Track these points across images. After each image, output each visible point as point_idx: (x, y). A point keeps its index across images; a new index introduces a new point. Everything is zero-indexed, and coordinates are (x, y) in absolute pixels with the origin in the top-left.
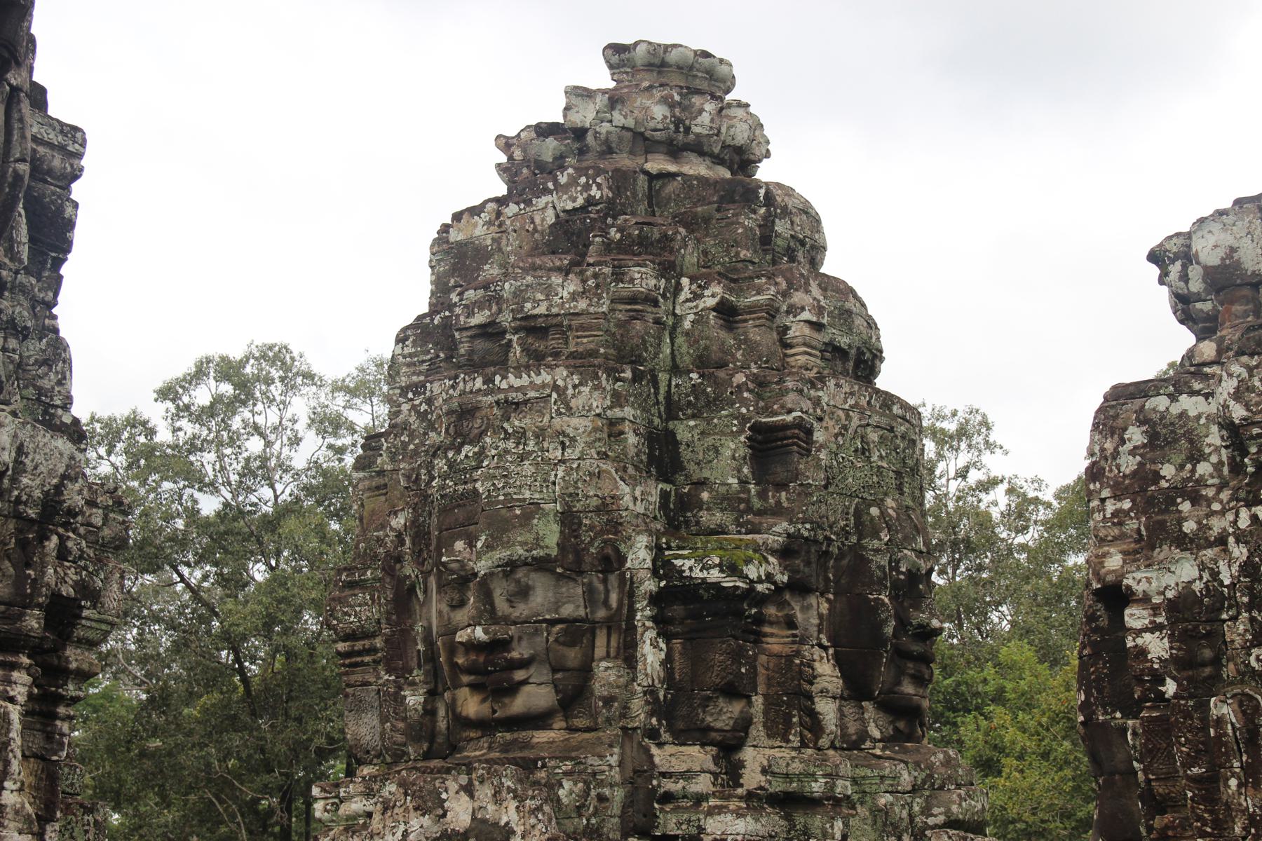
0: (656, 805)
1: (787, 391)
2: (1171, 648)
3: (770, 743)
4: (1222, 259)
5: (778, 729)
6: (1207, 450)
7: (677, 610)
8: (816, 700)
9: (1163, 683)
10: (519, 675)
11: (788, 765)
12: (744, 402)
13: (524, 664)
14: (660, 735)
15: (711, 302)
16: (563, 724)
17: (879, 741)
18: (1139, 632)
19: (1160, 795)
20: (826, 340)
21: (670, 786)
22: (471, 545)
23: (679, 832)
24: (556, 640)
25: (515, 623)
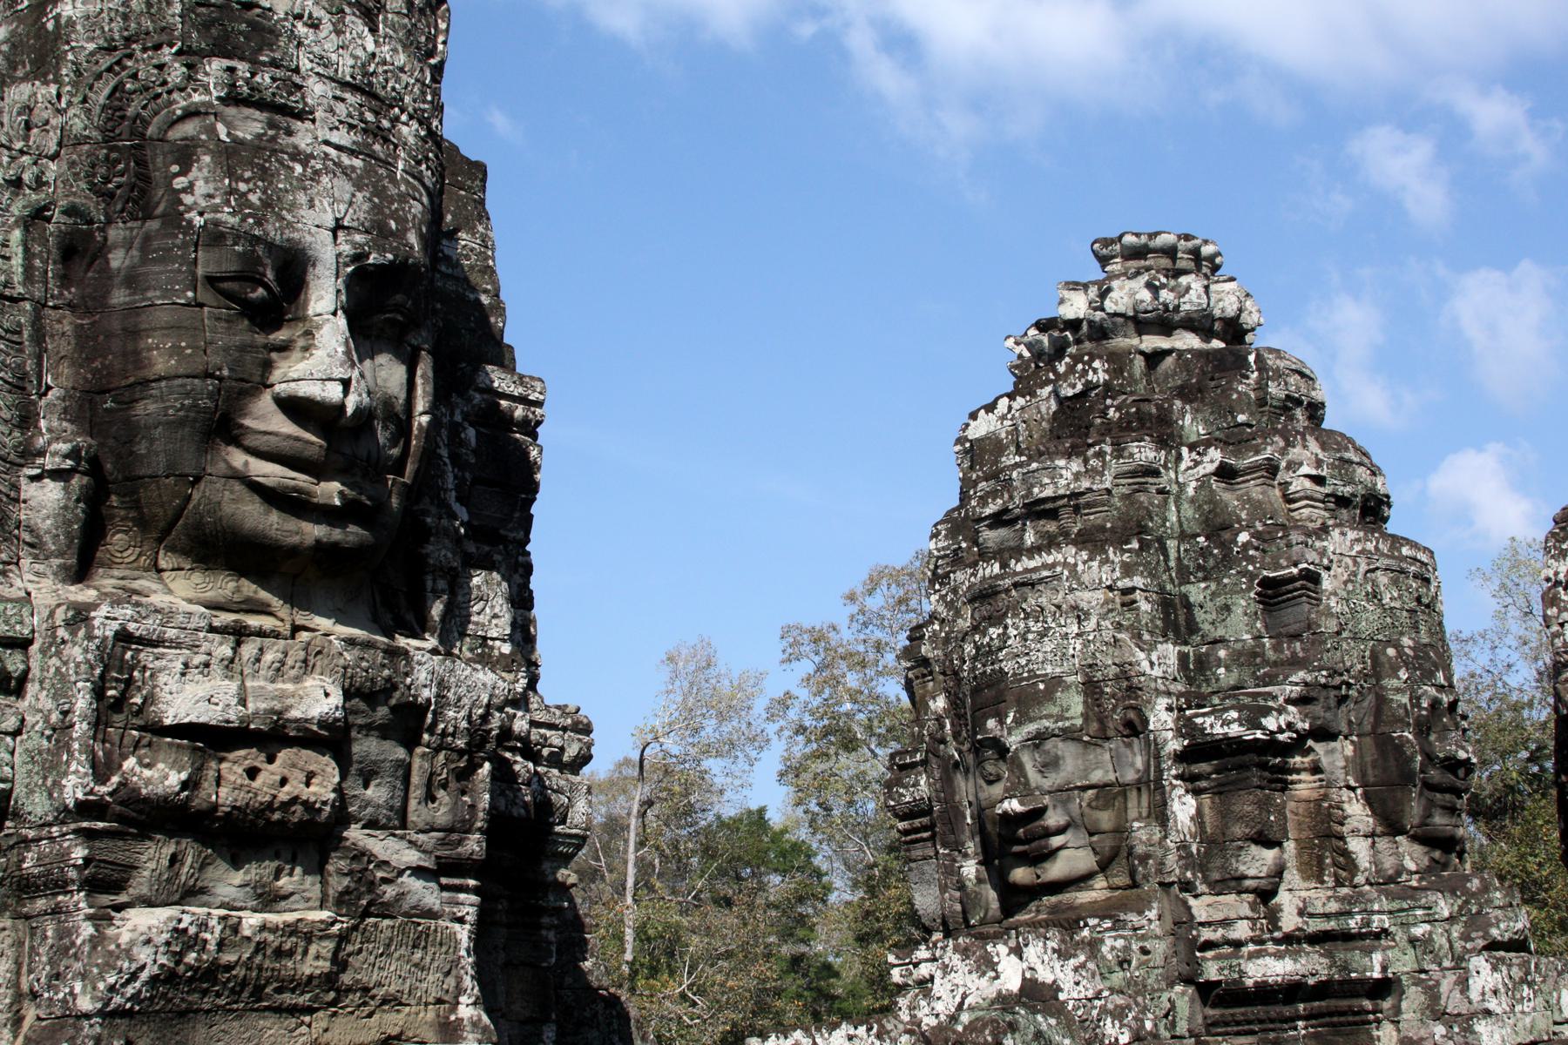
3: (1306, 885)
10: (1056, 841)
12: (1251, 560)
15: (1211, 468)
21: (1207, 934)
22: (1001, 722)
24: (1089, 805)
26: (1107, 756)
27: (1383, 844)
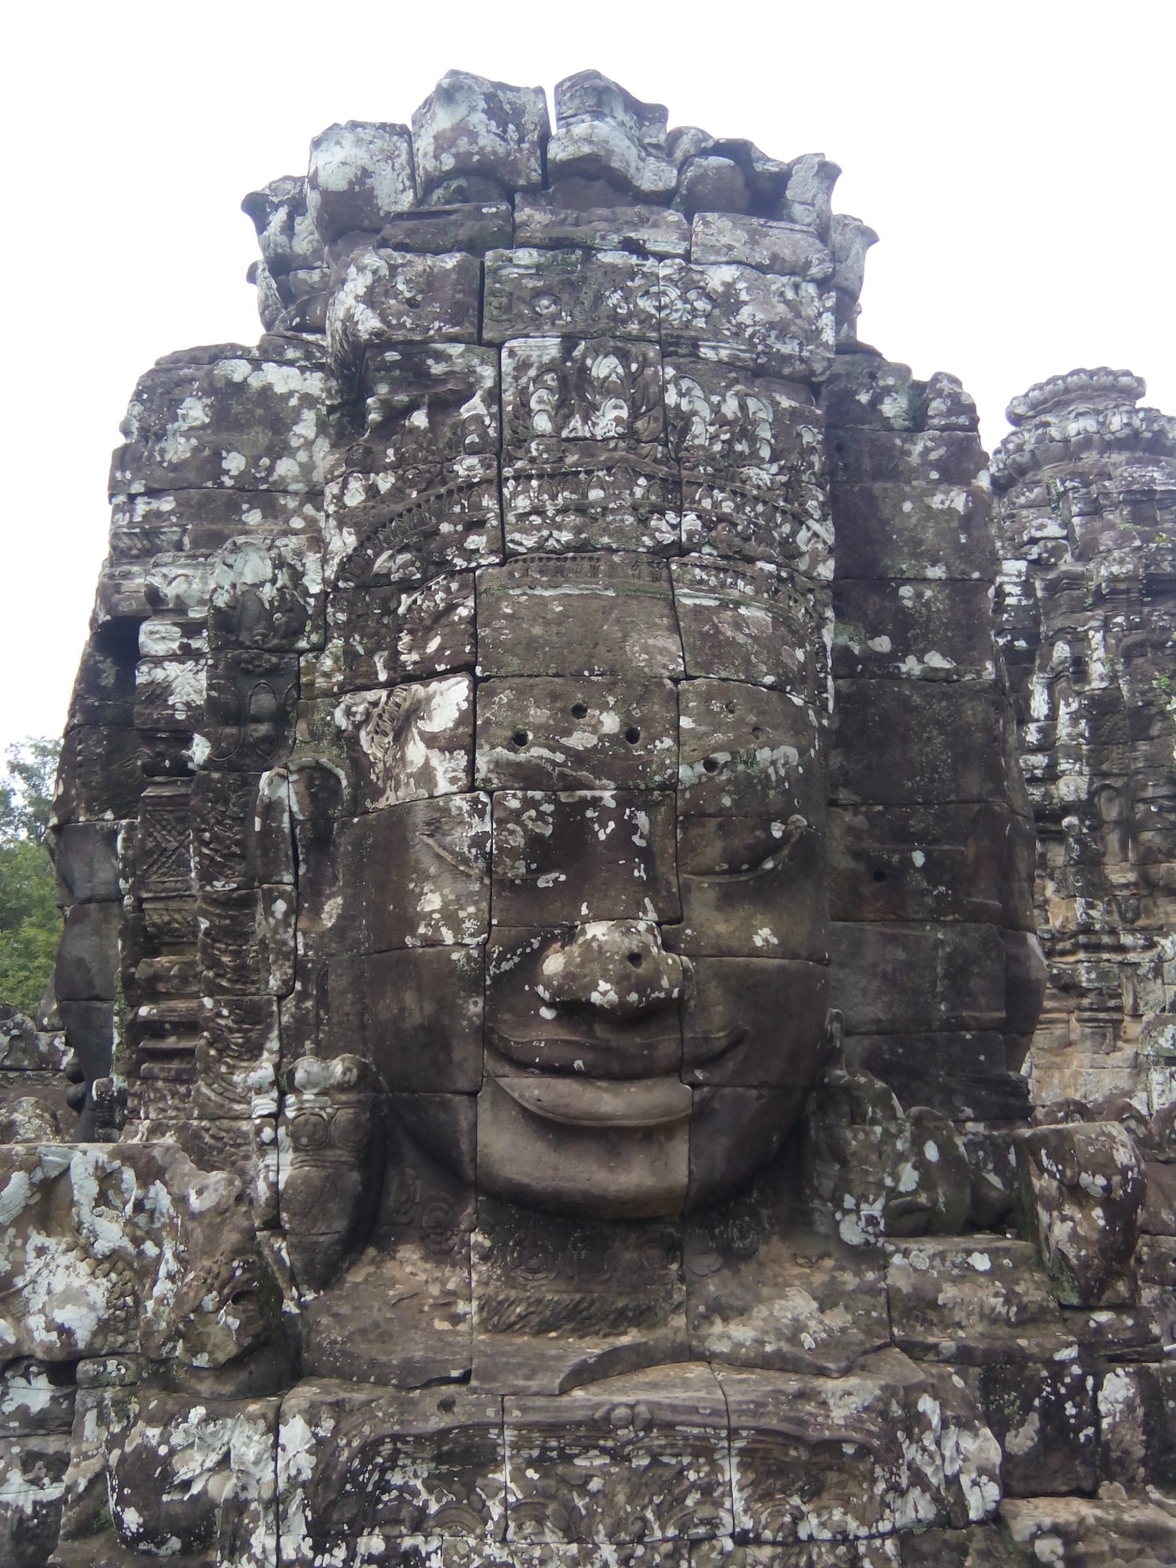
2: (211, 687)
4: (351, 183)
6: (295, 443)
9: (187, 742)
18: (158, 661)
19: (154, 925)
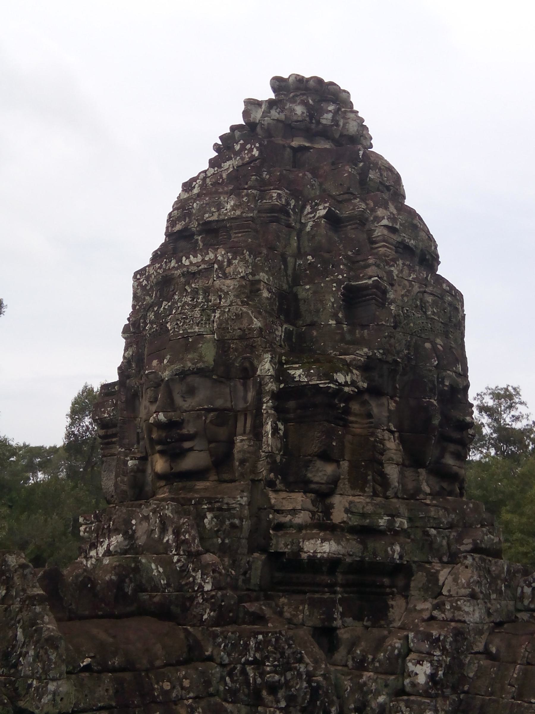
0: (271, 532)
1: (369, 266)
3: (352, 492)
5: (358, 483)
7: (291, 404)
8: (385, 465)
10: (187, 445)
11: (364, 507)
12: (341, 272)
13: (190, 438)
14: (276, 485)
15: (323, 212)
16: (215, 478)
17: (430, 494)
20: (399, 239)
23: (286, 550)
24: (211, 422)
25: (186, 411)
26: (228, 390)
27: (409, 473)
